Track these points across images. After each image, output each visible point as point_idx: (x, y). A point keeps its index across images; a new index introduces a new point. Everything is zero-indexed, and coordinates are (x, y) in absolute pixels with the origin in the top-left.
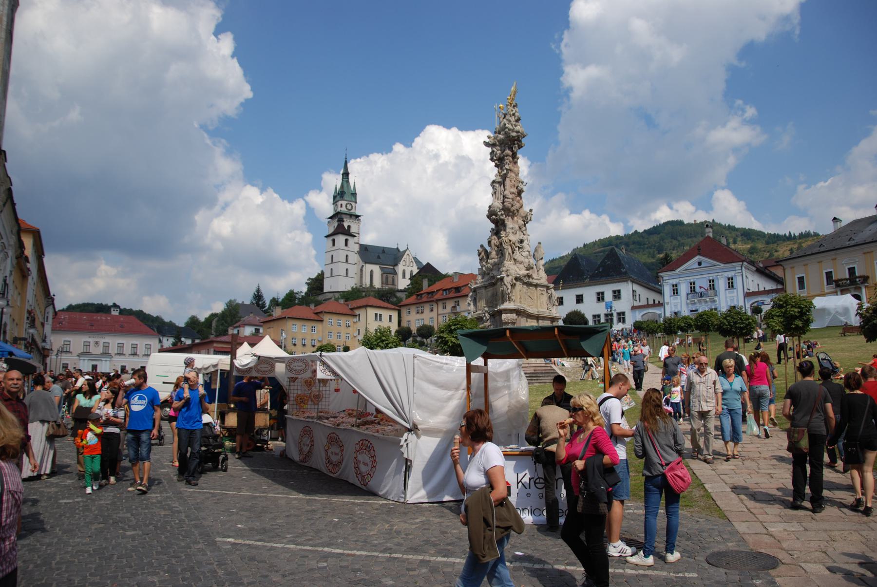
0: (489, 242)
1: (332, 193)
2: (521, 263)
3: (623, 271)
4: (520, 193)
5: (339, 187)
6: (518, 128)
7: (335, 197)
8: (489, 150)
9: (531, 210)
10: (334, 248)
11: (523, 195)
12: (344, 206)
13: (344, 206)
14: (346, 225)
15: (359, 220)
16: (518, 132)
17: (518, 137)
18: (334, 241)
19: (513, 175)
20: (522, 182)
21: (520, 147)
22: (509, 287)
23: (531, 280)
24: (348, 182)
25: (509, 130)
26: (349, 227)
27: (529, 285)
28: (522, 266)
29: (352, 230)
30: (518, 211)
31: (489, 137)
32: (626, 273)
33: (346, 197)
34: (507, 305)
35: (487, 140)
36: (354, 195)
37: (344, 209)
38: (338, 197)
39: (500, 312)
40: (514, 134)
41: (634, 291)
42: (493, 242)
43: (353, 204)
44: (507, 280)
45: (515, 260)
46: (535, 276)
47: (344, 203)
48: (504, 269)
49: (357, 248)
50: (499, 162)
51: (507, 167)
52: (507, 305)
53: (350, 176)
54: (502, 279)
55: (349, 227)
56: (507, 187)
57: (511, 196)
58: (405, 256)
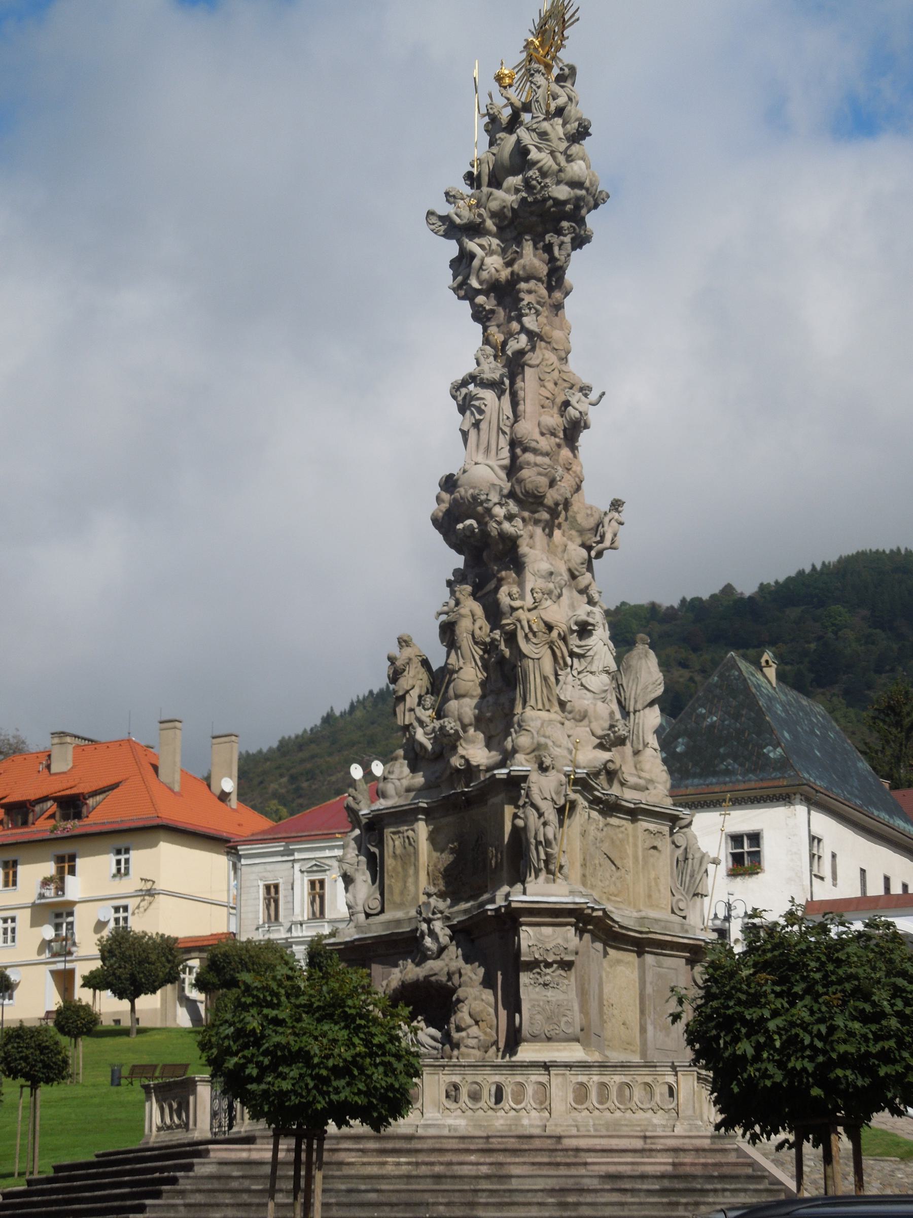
0: (448, 632)
2: (582, 717)
3: (774, 753)
4: (572, 431)
6: (577, 169)
8: (451, 249)
9: (616, 505)
11: (584, 438)
16: (575, 184)
17: (578, 203)
19: (552, 357)
20: (585, 390)
21: (580, 241)
22: (551, 815)
23: (615, 790)
25: (544, 174)
27: (609, 808)
28: (582, 732)
30: (567, 504)
31: (450, 197)
32: (783, 764)
34: (538, 891)
35: (445, 209)
39: (511, 919)
40: (562, 192)
41: (814, 839)
42: (464, 627)
44: (544, 788)
45: (562, 704)
46: (628, 773)
48: (524, 740)
50: (497, 302)
51: (530, 322)
52: (538, 891)
54: (516, 783)
56: (529, 406)
57: (545, 443)
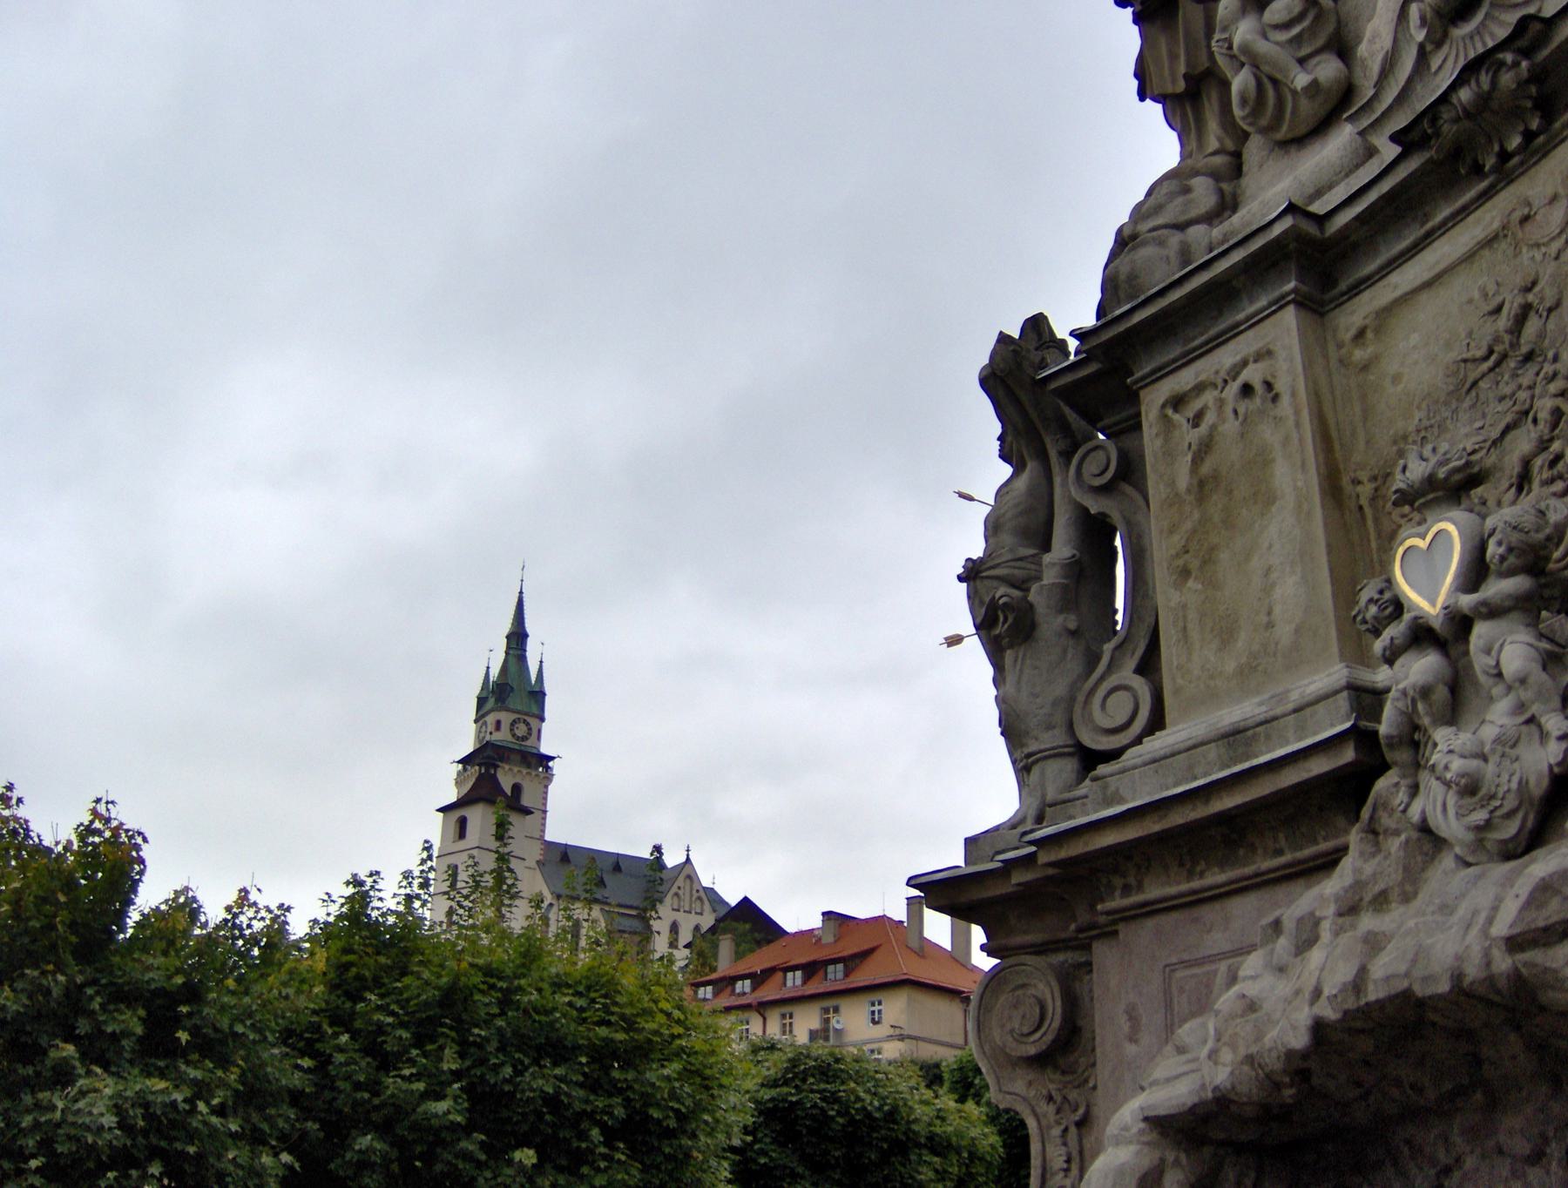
1: (476, 689)
5: (495, 672)
7: (481, 701)
10: (462, 845)
12: (505, 726)
13: (505, 726)
14: (506, 780)
15: (548, 768)
18: (462, 823)
24: (522, 658)
26: (517, 788)
29: (526, 801)
33: (513, 702)
36: (538, 696)
37: (502, 736)
38: (491, 703)
43: (533, 722)
47: (506, 718)
49: (534, 853)
53: (529, 641)
55: (517, 788)
58: (680, 882)
